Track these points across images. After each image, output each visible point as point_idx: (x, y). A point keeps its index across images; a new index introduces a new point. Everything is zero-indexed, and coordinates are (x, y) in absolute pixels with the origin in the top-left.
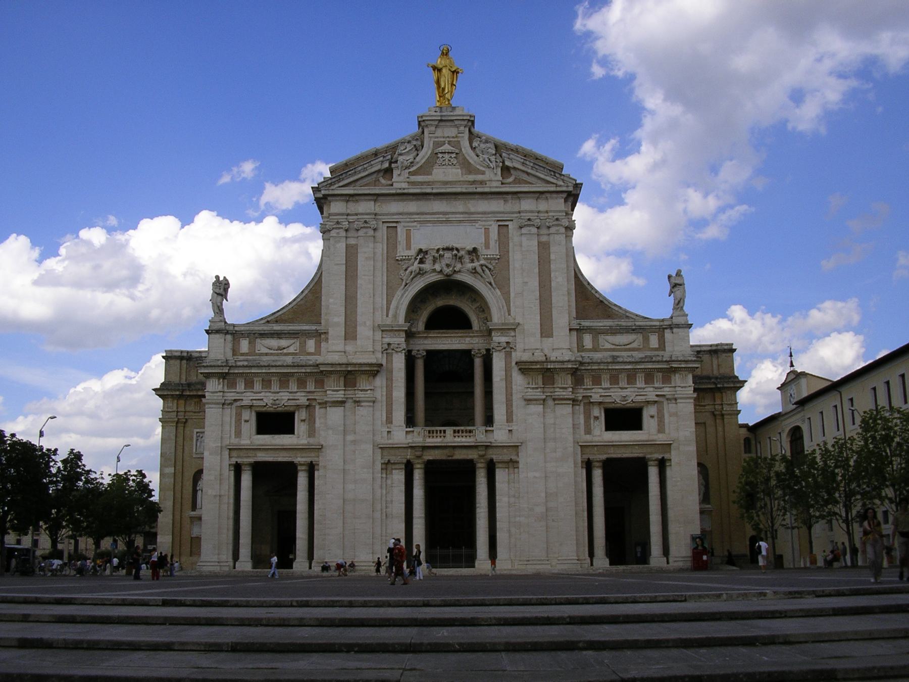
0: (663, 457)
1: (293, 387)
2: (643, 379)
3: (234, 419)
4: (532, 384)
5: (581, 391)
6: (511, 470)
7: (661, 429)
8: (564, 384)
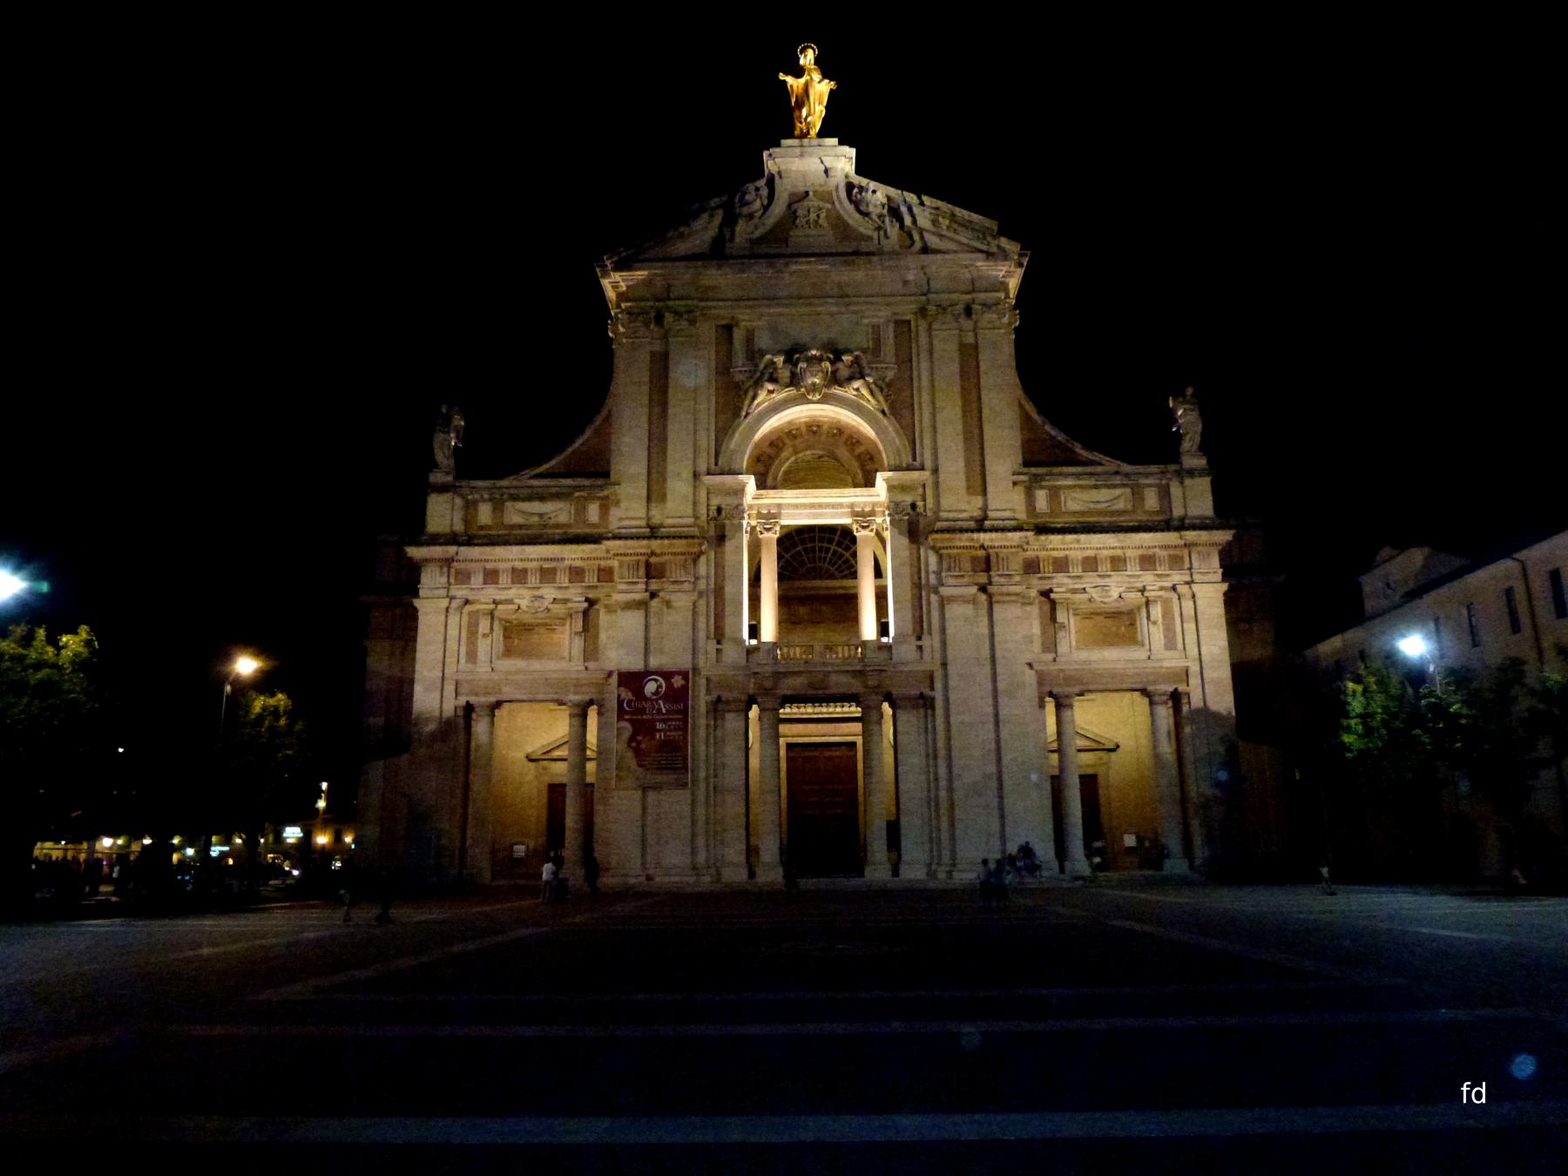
0: (1176, 689)
1: (563, 579)
2: (1137, 561)
3: (464, 634)
4: (955, 571)
5: (1035, 582)
6: (922, 711)
7: (1170, 644)
8: (1008, 570)
